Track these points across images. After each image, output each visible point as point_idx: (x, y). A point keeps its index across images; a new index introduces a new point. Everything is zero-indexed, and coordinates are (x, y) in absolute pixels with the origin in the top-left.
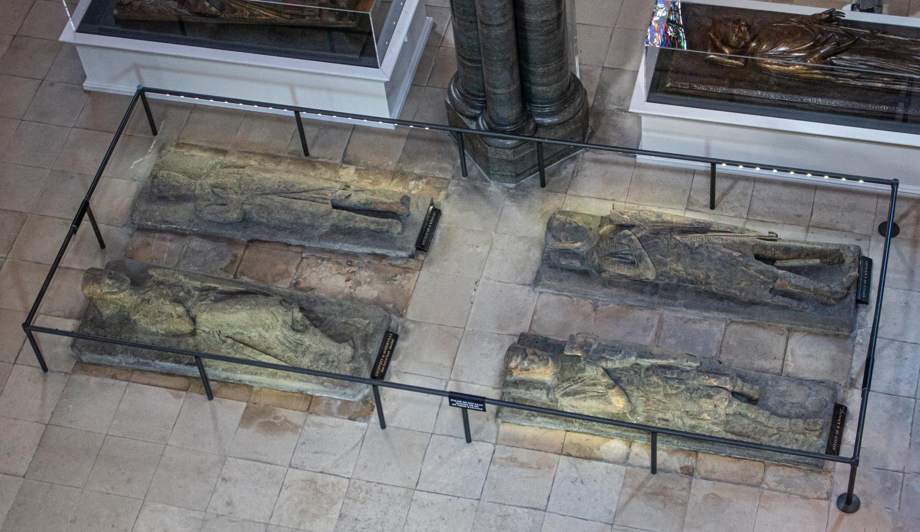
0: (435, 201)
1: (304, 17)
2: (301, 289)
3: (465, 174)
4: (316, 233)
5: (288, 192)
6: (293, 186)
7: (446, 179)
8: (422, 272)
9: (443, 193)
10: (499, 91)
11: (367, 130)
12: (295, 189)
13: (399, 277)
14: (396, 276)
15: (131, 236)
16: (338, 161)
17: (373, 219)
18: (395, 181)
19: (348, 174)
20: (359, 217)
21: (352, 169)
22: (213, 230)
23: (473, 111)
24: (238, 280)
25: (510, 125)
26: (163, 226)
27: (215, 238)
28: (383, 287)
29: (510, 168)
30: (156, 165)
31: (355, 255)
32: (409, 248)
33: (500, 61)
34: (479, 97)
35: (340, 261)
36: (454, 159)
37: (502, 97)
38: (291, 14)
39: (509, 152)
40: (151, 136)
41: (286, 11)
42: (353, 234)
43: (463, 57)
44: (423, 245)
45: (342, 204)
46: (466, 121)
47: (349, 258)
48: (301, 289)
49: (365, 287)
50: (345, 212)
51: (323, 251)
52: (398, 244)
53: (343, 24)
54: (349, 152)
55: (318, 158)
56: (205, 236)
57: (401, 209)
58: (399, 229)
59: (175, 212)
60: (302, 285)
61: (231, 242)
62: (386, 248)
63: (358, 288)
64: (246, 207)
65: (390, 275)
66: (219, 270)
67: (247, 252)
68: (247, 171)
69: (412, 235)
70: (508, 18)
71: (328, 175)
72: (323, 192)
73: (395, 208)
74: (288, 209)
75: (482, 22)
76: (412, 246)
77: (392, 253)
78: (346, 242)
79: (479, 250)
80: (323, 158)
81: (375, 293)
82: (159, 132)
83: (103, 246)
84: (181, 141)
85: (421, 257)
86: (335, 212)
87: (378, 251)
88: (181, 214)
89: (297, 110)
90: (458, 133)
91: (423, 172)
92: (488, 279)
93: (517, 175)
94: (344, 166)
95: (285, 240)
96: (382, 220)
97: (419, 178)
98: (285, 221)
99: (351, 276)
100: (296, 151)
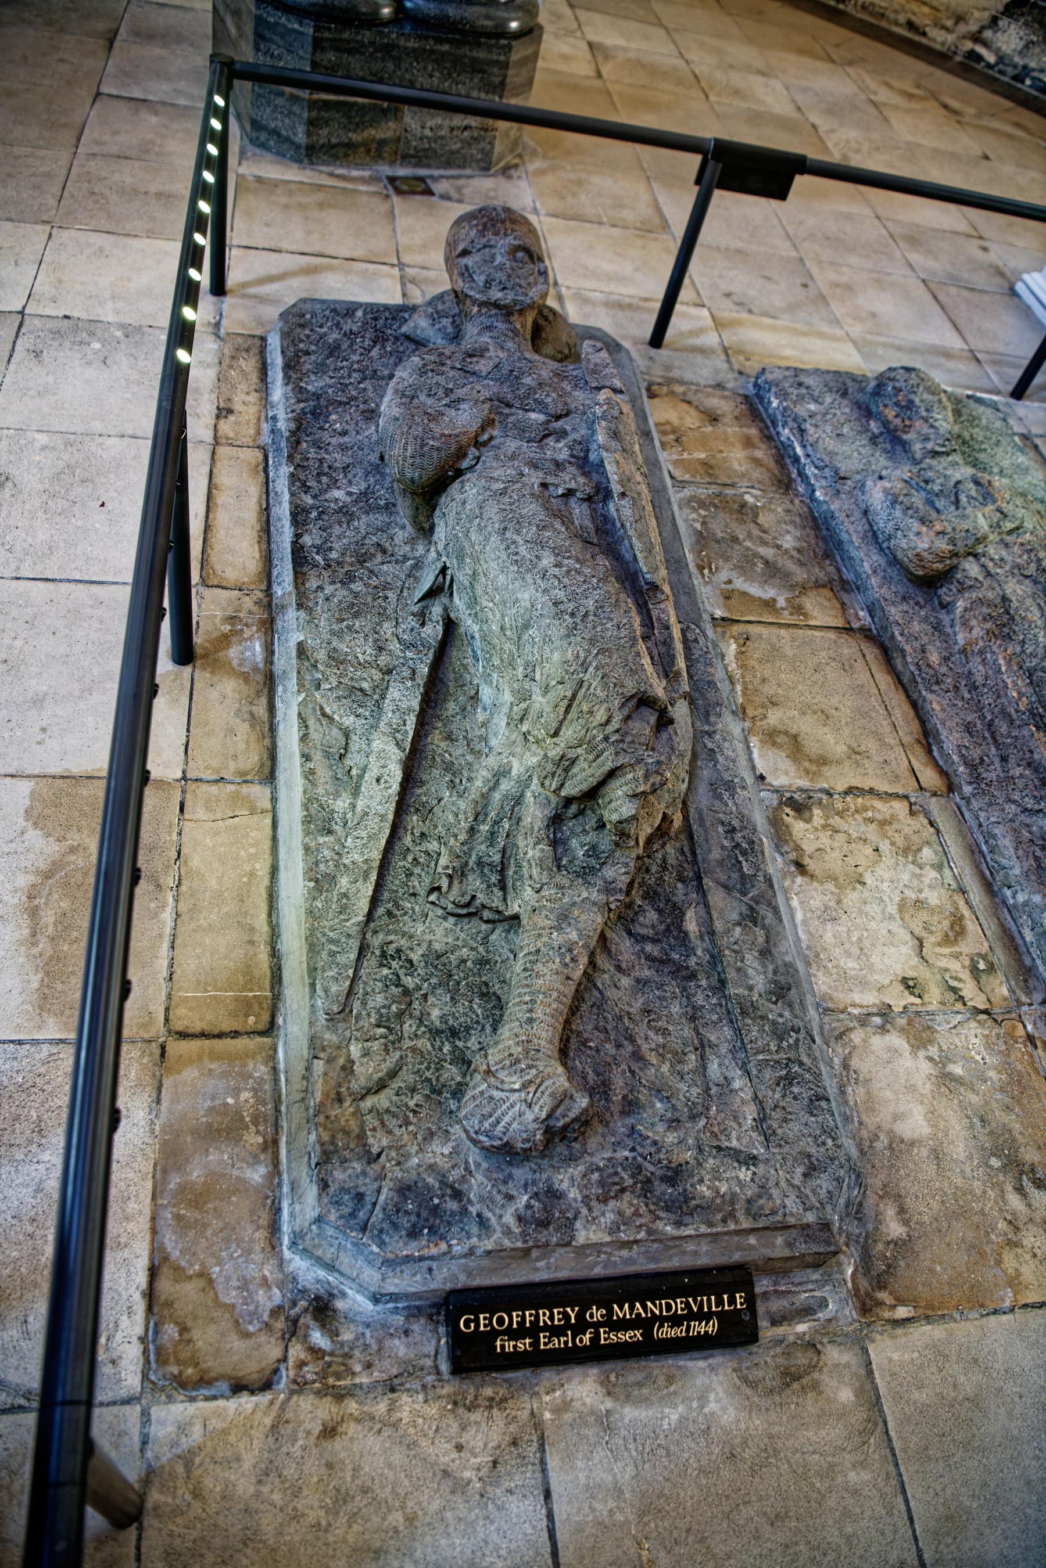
28: (959, 1148)
35: (971, 926)
47: (1000, 957)
49: (918, 1068)
60: (798, 827)
63: (896, 1040)
67: (832, 635)
81: (915, 1124)
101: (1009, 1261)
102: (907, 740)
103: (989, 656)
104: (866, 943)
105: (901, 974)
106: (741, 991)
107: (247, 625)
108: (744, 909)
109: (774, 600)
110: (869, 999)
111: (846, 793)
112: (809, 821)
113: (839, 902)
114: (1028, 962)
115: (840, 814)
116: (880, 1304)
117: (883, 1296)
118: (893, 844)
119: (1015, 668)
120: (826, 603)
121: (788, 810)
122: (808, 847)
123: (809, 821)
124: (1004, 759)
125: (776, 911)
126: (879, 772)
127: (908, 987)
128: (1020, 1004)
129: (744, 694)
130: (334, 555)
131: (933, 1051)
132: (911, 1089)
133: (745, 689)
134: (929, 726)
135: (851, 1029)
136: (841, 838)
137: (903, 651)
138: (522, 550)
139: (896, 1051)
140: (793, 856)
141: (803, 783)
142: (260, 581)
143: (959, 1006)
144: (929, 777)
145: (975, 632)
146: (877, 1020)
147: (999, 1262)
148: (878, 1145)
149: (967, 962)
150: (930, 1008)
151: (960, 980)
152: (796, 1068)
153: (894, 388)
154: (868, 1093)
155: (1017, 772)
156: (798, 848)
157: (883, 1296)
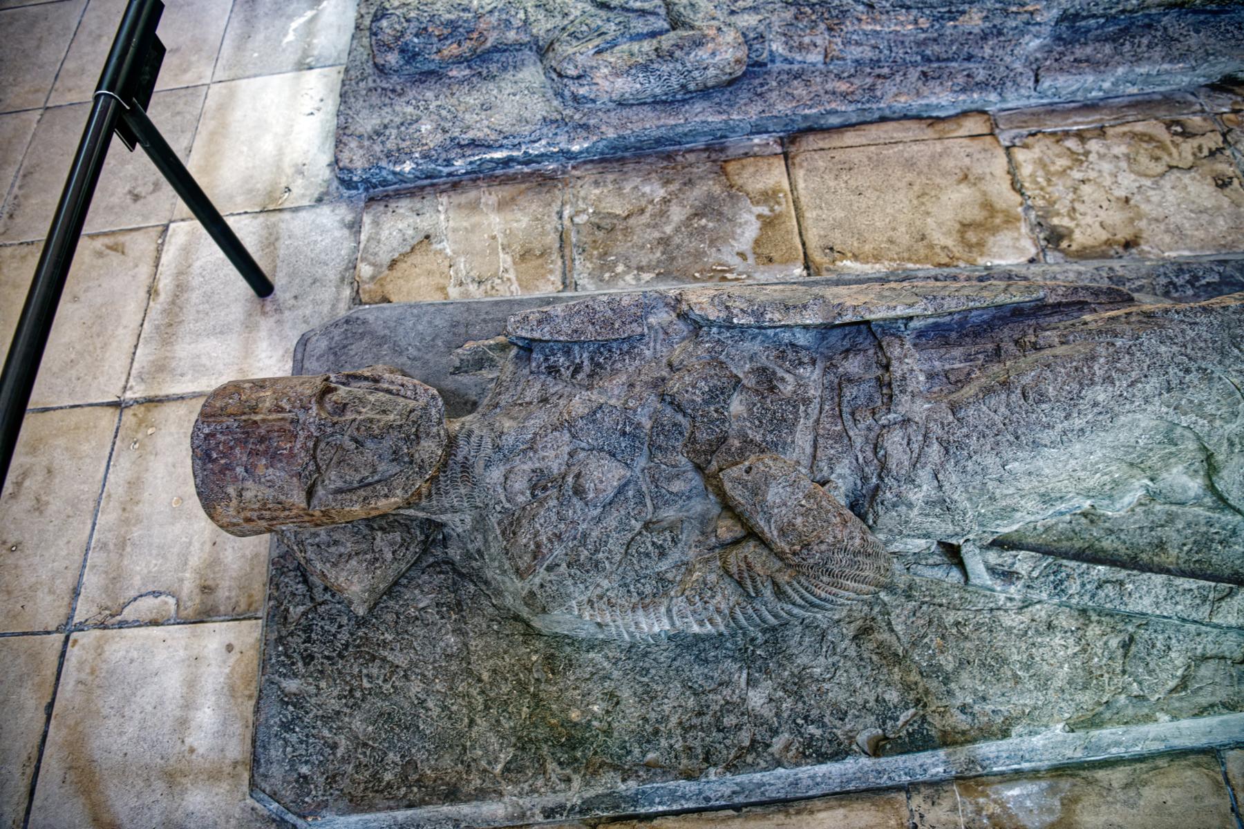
15: (354, 227)
24: (826, 275)
26: (460, 165)
35: (1139, 127)
60: (1080, 239)
61: (717, 151)
67: (800, 174)
83: (261, 285)
95: (916, 104)
102: (930, 133)
103: (855, 37)
104: (1194, 207)
105: (1212, 188)
107: (979, 811)
109: (759, 216)
113: (1157, 220)
114: (1159, 97)
119: (884, 17)
120: (752, 169)
121: (1064, 244)
122: (1104, 236)
123: (1071, 232)
124: (969, 58)
130: (893, 696)
133: (910, 260)
138: (1078, 423)
140: (1120, 250)
141: (1024, 229)
142: (889, 802)
144: (974, 125)
145: (819, 42)
153: (417, 35)
155: (987, 51)
156: (1108, 243)
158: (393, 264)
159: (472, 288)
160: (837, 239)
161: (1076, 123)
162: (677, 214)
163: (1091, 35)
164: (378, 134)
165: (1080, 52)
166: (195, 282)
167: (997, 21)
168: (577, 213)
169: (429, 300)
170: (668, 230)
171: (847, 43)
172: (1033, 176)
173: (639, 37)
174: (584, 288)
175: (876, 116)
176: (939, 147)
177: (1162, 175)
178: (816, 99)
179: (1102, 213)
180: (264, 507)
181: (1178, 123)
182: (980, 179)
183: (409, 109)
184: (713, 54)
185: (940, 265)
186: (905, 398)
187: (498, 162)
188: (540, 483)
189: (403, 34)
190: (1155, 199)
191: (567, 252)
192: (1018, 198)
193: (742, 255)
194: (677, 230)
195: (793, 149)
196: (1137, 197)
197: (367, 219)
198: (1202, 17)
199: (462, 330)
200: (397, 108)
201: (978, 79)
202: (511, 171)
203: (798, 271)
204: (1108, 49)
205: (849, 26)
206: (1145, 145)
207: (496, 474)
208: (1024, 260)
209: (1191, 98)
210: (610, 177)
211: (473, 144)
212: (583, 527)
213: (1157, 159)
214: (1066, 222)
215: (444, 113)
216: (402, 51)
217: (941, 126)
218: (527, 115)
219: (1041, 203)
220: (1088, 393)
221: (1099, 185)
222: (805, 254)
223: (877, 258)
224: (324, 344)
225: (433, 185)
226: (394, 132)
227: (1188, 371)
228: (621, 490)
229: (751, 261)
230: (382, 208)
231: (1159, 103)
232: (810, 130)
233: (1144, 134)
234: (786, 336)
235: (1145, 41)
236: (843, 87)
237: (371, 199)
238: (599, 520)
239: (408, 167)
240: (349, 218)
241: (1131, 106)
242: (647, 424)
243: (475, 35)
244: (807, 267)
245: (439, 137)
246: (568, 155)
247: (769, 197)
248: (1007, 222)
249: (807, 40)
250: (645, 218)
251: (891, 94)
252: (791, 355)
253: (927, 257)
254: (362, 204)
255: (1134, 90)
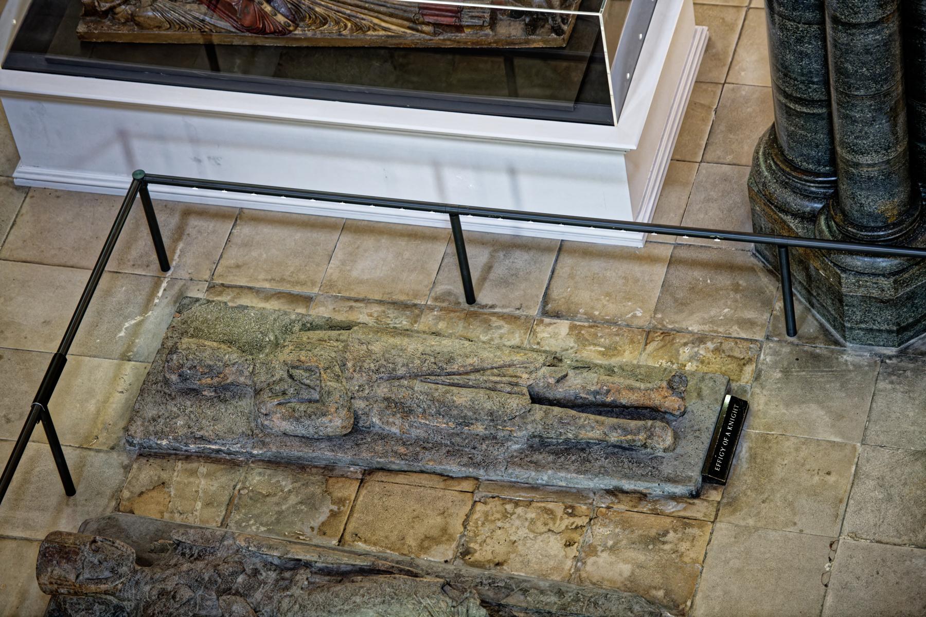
0: (734, 385)
1: (459, 28)
2: (474, 565)
3: (792, 330)
4: (499, 453)
5: (439, 372)
6: (450, 360)
7: (752, 341)
8: (718, 525)
9: (749, 369)
10: (863, 160)
11: (588, 252)
12: (455, 367)
13: (671, 536)
14: (666, 533)
15: (127, 468)
16: (535, 312)
17: (615, 420)
18: (650, 348)
19: (556, 336)
20: (585, 418)
21: (563, 326)
22: (296, 451)
23: (806, 203)
24: (346, 548)
25: (886, 227)
26: (192, 447)
27: (298, 466)
28: (641, 557)
29: (888, 314)
30: (172, 328)
31: (580, 495)
32: (690, 479)
33: (873, 97)
34: (819, 175)
35: (550, 506)
36: (767, 304)
37: (874, 172)
38: (436, 25)
39: (886, 283)
40: (160, 274)
41: (427, 19)
42: (573, 451)
43: (787, 96)
44: (717, 469)
45: (550, 395)
46: (793, 223)
47: (569, 501)
48: (474, 565)
49: (604, 558)
50: (556, 410)
51: (513, 486)
52: (667, 469)
53: (538, 41)
54: (555, 293)
55: (492, 307)
56: (274, 463)
57: (671, 403)
58: (669, 440)
59: (215, 420)
60: (477, 556)
61: (329, 470)
62: (643, 477)
63: (591, 560)
64: (359, 404)
65: (653, 533)
66: (308, 531)
67: (364, 492)
68: (357, 334)
69: (696, 451)
70: (890, 9)
71: (516, 340)
72: (511, 371)
73: (656, 399)
74: (444, 409)
75: (836, 20)
76: (695, 474)
77: (655, 488)
78: (562, 468)
79: (831, 479)
80: (503, 307)
81: (626, 569)
82: (173, 264)
83: (70, 489)
84: (219, 281)
85: (715, 495)
86: (539, 411)
87: (627, 485)
88: (225, 423)
89: (455, 213)
90: (781, 246)
91: (707, 328)
92: (855, 536)
93: (901, 330)
94: (547, 320)
95: (439, 468)
96: (633, 424)
97: (701, 339)
98: (438, 431)
99: (576, 536)
100: (449, 293)
101: (687, 559)
102: (442, 485)
104: (544, 553)
105: (562, 545)
106: (556, 606)
108: (521, 593)
109: (331, 510)
110: (569, 563)
111: (465, 528)
112: (476, 551)
113: (521, 556)
114: (575, 491)
115: (476, 535)
116: (683, 609)
117: (681, 607)
118: (499, 520)
120: (340, 485)
121: (467, 557)
122: (490, 557)
123: (476, 551)
124: (474, 448)
125: (525, 581)
126: (458, 507)
127: (569, 545)
128: (591, 504)
129: (393, 550)
131: (600, 548)
132: (611, 564)
133: (390, 549)
134: (439, 472)
135: (580, 576)
136: (488, 540)
137: (391, 462)
138: (346, 608)
139: (595, 563)
140: (492, 565)
141: (454, 545)
143: (585, 529)
144: (467, 486)
145: (397, 423)
146: (579, 564)
147: (686, 563)
148: (629, 586)
149: (566, 516)
150: (581, 541)
151: (573, 523)
152: (592, 600)
153: (190, 369)
154: (608, 580)
155: (484, 446)
156: (489, 561)
157: (681, 607)
158: (142, 493)
159: (177, 515)
160: (364, 532)
161: (520, 496)
162: (293, 499)
163: (547, 449)
164: (154, 420)
165: (537, 457)
166: (34, 479)
167: (493, 432)
168: (243, 488)
169: (153, 517)
170: (284, 507)
171: (411, 426)
172: (477, 520)
173: (302, 401)
174: (230, 528)
175: (418, 469)
176: (441, 494)
177: (541, 534)
178: (385, 454)
179: (497, 546)
180: (59, 579)
181: (572, 507)
182: (450, 515)
183: (175, 409)
184: (330, 421)
185: (403, 554)
186: (295, 588)
187: (213, 450)
188: (162, 593)
189: (182, 366)
190: (528, 545)
191: (230, 507)
192: (462, 529)
193: (312, 528)
194: (288, 509)
195: (368, 478)
196: (521, 542)
197: (135, 466)
198: (616, 450)
199: (160, 533)
200: (169, 407)
201: (475, 461)
202: (220, 456)
203: (335, 542)
204: (551, 458)
205: (412, 418)
206: (546, 516)
207: (148, 588)
208: (443, 560)
209: (591, 495)
210: (269, 472)
211: (202, 438)
212: (171, 610)
213: (546, 524)
214: (477, 547)
215: (192, 416)
216: (180, 376)
217: (450, 482)
218: (235, 429)
219: (471, 534)
220: (354, 598)
221: (507, 532)
222: (343, 535)
223: (375, 544)
224: (95, 526)
225: (176, 454)
226: (163, 421)
227: (393, 598)
228: (188, 601)
229: (315, 532)
230: (145, 461)
231: (573, 494)
232: (382, 469)
233: (549, 510)
234: (270, 559)
235: (573, 458)
236: (402, 450)
237: (141, 455)
238: (177, 609)
239: (164, 442)
240: (126, 462)
241: (556, 492)
242: (207, 579)
243: (222, 376)
244: (340, 541)
245: (185, 430)
246: (252, 456)
247: (341, 501)
248: (448, 540)
249: (391, 420)
250: (275, 499)
251: (427, 459)
252: (269, 566)
253: (398, 549)
254: (135, 456)
255: (563, 484)
